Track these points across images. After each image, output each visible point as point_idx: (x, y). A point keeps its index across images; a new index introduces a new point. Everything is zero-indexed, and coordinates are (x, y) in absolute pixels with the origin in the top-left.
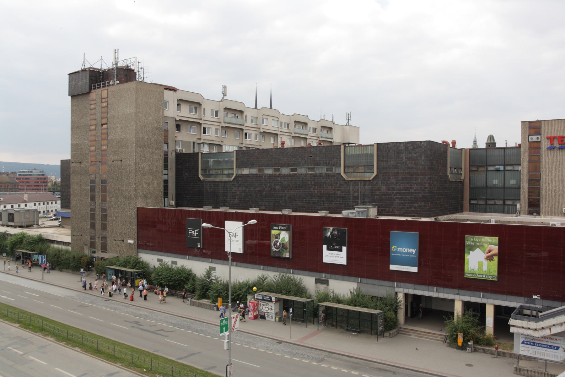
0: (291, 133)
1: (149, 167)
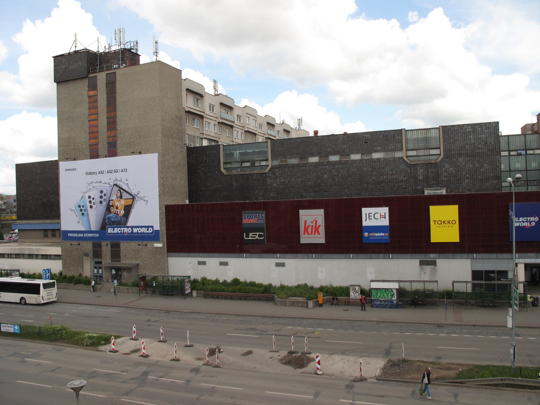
0: (265, 134)
1: (173, 160)
